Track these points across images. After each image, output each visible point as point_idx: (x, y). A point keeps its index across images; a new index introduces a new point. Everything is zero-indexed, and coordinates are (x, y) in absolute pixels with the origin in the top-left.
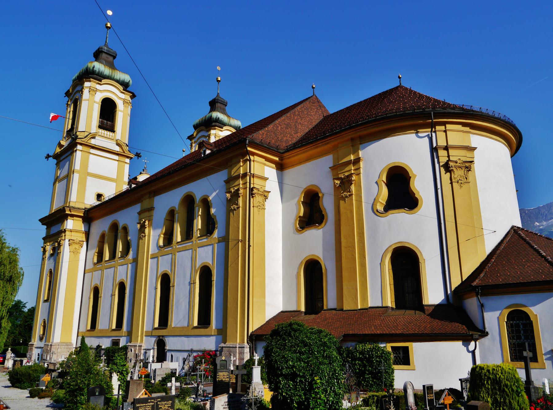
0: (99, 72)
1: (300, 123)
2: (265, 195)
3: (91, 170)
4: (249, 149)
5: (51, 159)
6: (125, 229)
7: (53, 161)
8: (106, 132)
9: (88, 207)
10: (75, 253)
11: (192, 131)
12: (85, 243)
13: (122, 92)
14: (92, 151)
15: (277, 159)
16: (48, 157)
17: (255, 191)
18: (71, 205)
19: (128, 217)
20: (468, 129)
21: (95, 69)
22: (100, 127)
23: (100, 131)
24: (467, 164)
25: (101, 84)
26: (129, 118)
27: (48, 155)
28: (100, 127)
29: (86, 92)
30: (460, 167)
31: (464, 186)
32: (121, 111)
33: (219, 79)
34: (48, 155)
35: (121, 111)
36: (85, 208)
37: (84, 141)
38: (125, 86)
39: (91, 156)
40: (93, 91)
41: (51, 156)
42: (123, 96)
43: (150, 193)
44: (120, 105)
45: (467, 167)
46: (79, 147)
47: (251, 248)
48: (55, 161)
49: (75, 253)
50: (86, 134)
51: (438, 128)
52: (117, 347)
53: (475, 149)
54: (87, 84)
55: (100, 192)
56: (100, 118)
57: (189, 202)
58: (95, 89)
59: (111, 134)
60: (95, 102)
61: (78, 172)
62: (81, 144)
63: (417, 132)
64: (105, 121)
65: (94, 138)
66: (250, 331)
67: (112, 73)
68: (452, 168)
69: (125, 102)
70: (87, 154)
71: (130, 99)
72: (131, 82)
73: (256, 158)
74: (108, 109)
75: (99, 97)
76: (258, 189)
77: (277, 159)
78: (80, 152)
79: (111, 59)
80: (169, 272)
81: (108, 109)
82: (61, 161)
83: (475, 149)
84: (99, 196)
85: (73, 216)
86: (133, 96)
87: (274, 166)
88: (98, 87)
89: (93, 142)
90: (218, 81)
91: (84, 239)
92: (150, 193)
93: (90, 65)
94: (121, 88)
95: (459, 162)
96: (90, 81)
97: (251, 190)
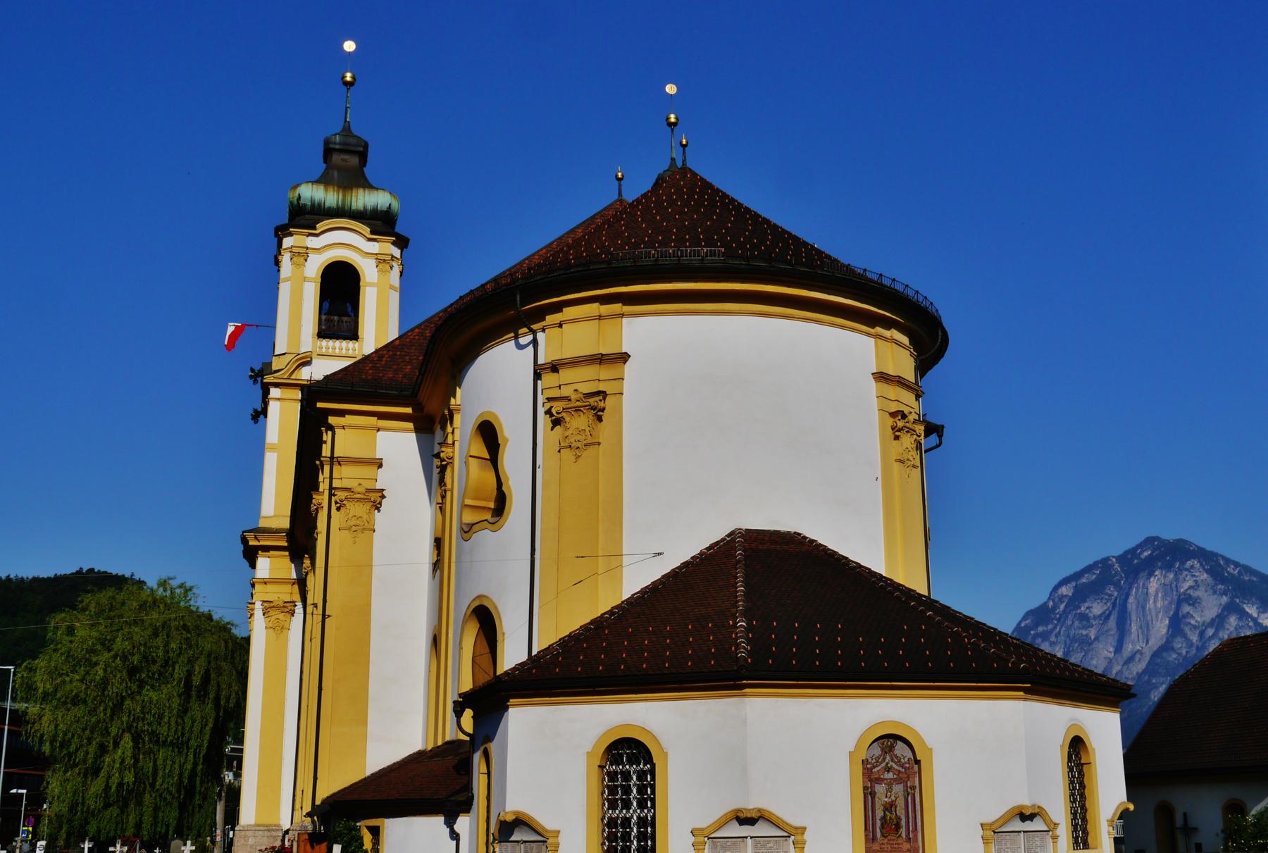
0: (313, 204)
2: (375, 499)
4: (320, 405)
8: (337, 343)
10: (278, 629)
12: (300, 605)
13: (370, 240)
15: (409, 410)
18: (263, 524)
20: (617, 307)
21: (302, 202)
22: (322, 334)
23: (324, 342)
24: (592, 401)
26: (395, 298)
27: (255, 411)
28: (322, 334)
29: (285, 259)
30: (577, 410)
31: (588, 454)
32: (371, 285)
33: (673, 120)
35: (371, 285)
37: (281, 377)
38: (380, 223)
40: (302, 254)
42: (374, 247)
44: (368, 271)
45: (594, 408)
46: (274, 392)
49: (278, 629)
50: (288, 358)
51: (551, 319)
53: (624, 357)
54: (287, 242)
58: (303, 251)
59: (351, 344)
60: (305, 279)
61: (274, 448)
62: (277, 385)
63: (516, 337)
65: (308, 363)
66: (322, 794)
67: (344, 200)
68: (579, 409)
69: (381, 260)
71: (396, 252)
72: (396, 205)
73: (349, 419)
74: (340, 288)
75: (315, 266)
77: (409, 410)
78: (278, 403)
79: (354, 161)
81: (340, 288)
83: (624, 357)
85: (266, 549)
86: (402, 242)
87: (410, 425)
88: (312, 242)
90: (670, 124)
91: (297, 597)
93: (292, 196)
94: (366, 230)
95: (573, 397)
96: (291, 234)
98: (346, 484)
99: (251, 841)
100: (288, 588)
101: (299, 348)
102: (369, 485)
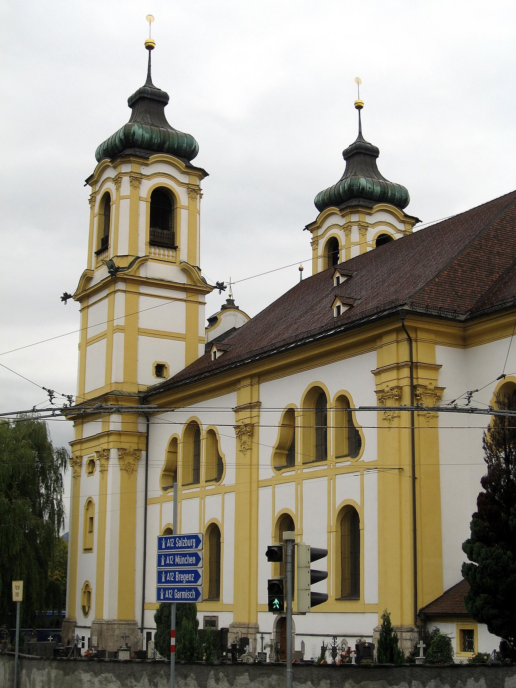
0: (143, 140)
1: (498, 253)
3: (144, 323)
5: (70, 301)
6: (212, 433)
7: (74, 305)
9: (143, 389)
11: (314, 214)
12: (144, 453)
13: (183, 173)
14: (143, 289)
16: (66, 297)
17: (419, 391)
19: (217, 413)
23: (153, 250)
25: (147, 165)
27: (66, 294)
28: (153, 243)
32: (184, 208)
34: (66, 294)
35: (184, 208)
36: (139, 392)
39: (142, 298)
40: (137, 179)
41: (70, 296)
43: (251, 377)
47: (417, 482)
48: (78, 305)
50: (131, 259)
52: (213, 628)
55: (161, 361)
56: (151, 226)
57: (317, 396)
60: (140, 199)
62: (124, 280)
64: (160, 231)
70: (136, 296)
75: (146, 188)
76: (425, 387)
78: (123, 294)
80: (293, 512)
82: (88, 307)
84: (160, 369)
89: (143, 273)
92: (251, 377)
97: (413, 388)
98: (421, 382)
99: (117, 633)
100: (135, 439)
101: (137, 251)
102: (434, 384)
